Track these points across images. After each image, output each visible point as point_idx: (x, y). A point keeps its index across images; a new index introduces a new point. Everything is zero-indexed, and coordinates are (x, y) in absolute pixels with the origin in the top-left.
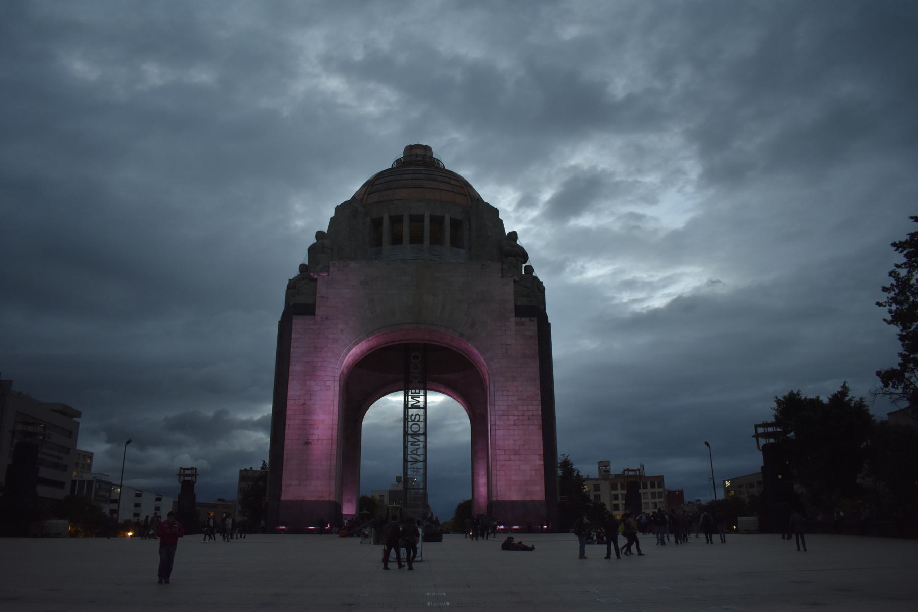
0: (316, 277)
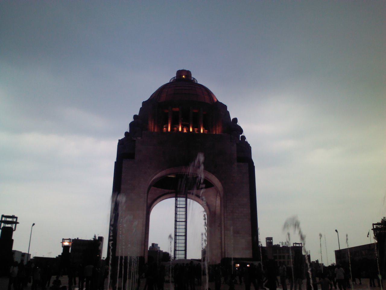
0: (135, 139)
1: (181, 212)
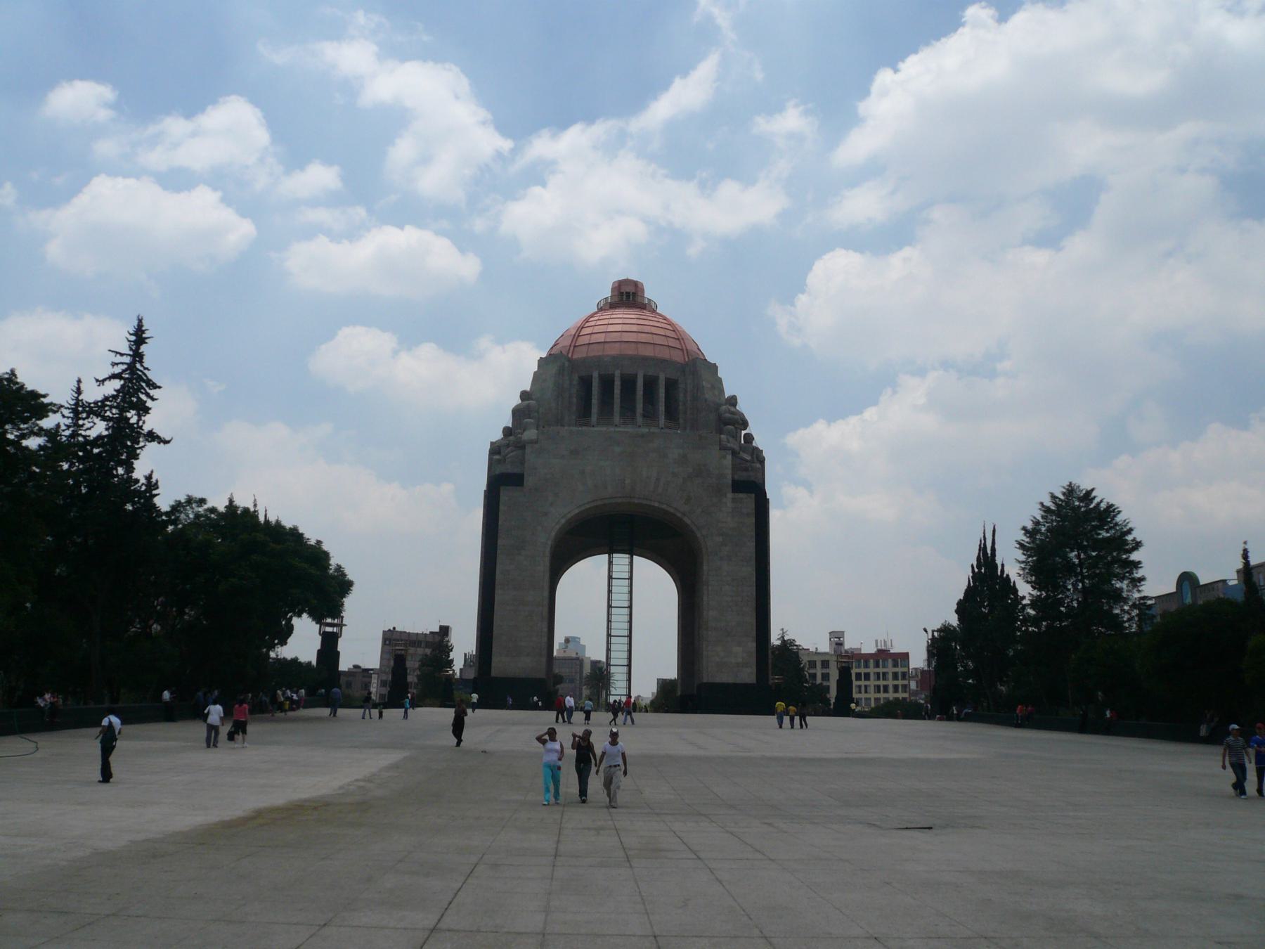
1: (620, 588)
